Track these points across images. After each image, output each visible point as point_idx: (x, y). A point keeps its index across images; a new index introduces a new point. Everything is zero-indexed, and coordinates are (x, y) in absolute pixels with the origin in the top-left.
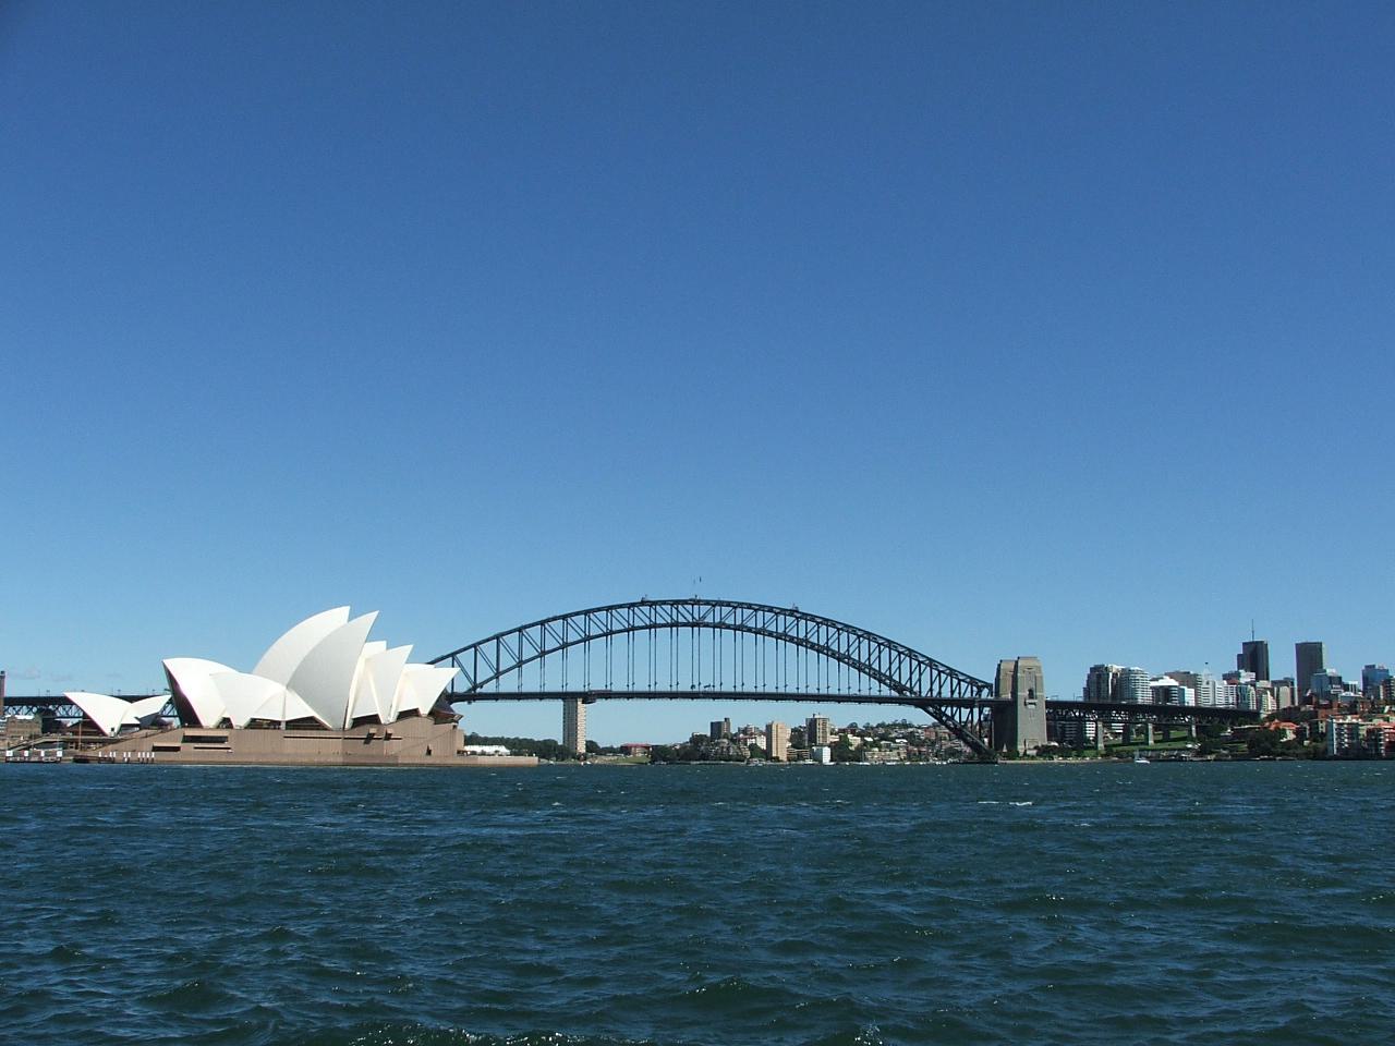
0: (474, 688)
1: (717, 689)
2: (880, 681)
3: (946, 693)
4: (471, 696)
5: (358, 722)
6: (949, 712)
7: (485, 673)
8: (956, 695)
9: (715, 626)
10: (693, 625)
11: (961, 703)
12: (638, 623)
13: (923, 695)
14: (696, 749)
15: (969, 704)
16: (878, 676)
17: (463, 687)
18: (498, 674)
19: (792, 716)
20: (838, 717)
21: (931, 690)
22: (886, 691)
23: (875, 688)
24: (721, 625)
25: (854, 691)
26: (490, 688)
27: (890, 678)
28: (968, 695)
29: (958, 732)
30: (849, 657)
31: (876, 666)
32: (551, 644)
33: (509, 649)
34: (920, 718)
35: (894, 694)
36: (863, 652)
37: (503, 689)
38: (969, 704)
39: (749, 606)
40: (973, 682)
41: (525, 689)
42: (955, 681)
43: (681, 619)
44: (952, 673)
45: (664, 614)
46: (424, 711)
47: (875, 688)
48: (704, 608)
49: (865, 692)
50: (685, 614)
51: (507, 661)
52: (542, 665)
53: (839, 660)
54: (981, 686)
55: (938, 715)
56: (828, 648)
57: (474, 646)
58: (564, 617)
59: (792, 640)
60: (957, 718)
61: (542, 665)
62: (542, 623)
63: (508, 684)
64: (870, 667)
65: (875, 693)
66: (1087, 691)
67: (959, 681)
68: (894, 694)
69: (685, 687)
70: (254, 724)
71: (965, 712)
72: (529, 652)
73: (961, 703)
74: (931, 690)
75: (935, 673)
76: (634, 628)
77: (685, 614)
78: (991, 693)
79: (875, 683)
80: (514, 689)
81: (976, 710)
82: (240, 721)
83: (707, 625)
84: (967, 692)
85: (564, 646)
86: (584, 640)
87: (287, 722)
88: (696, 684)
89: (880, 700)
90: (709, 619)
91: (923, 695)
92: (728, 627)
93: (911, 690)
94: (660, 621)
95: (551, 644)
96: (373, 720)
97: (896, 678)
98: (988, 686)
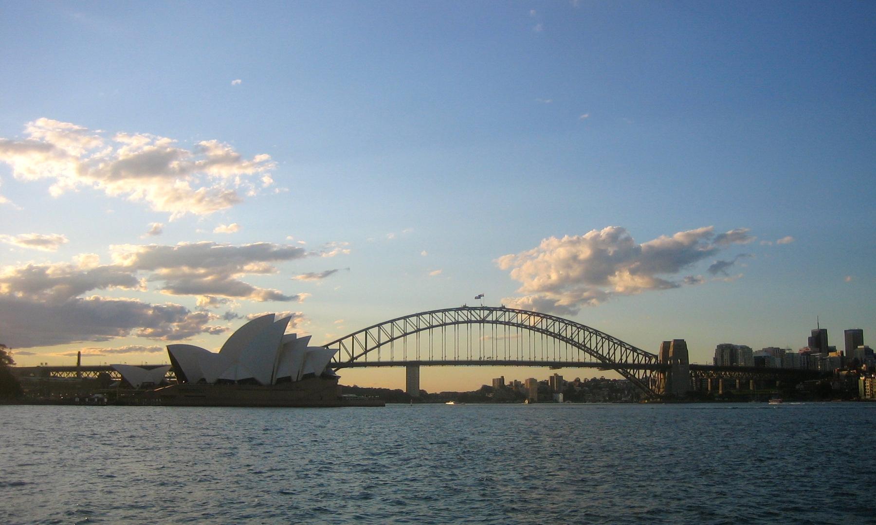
0: (353, 358)
1: (495, 359)
2: (591, 354)
3: (630, 361)
4: (351, 364)
5: (280, 381)
6: (632, 372)
7: (358, 351)
8: (636, 362)
9: (493, 322)
10: (479, 322)
11: (639, 367)
12: (448, 321)
13: (617, 361)
14: (483, 396)
15: (645, 367)
17: (345, 358)
18: (366, 352)
19: (543, 374)
20: (569, 375)
21: (621, 359)
22: (594, 360)
23: (588, 358)
24: (497, 322)
25: (575, 360)
26: (362, 359)
27: (597, 352)
28: (643, 362)
30: (572, 340)
31: (588, 345)
33: (373, 338)
34: (612, 375)
35: (599, 361)
36: (581, 337)
37: (369, 360)
38: (645, 367)
39: (513, 311)
40: (646, 354)
41: (382, 360)
42: (635, 354)
43: (473, 319)
44: (634, 350)
45: (463, 315)
46: (319, 373)
47: (588, 358)
48: (487, 312)
49: (582, 360)
50: (476, 315)
51: (371, 344)
52: (392, 346)
53: (567, 342)
55: (625, 374)
56: (560, 335)
57: (353, 335)
58: (405, 318)
59: (538, 330)
60: (637, 376)
61: (392, 346)
62: (392, 321)
63: (372, 357)
64: (585, 346)
65: (588, 360)
66: (715, 359)
67: (638, 354)
68: (599, 361)
69: (476, 358)
70: (220, 382)
71: (642, 372)
72: (384, 338)
73: (639, 367)
74: (621, 359)
75: (623, 349)
76: (445, 324)
77: (476, 315)
78: (657, 359)
79: (587, 355)
80: (376, 360)
81: (648, 372)
82: (211, 379)
83: (488, 322)
84: (643, 360)
85: (405, 334)
86: (416, 331)
87: (239, 381)
88: (482, 356)
90: (489, 318)
91: (617, 361)
92: (501, 323)
93: (609, 359)
94: (461, 320)
96: (288, 379)
97: (600, 352)
98: (656, 357)
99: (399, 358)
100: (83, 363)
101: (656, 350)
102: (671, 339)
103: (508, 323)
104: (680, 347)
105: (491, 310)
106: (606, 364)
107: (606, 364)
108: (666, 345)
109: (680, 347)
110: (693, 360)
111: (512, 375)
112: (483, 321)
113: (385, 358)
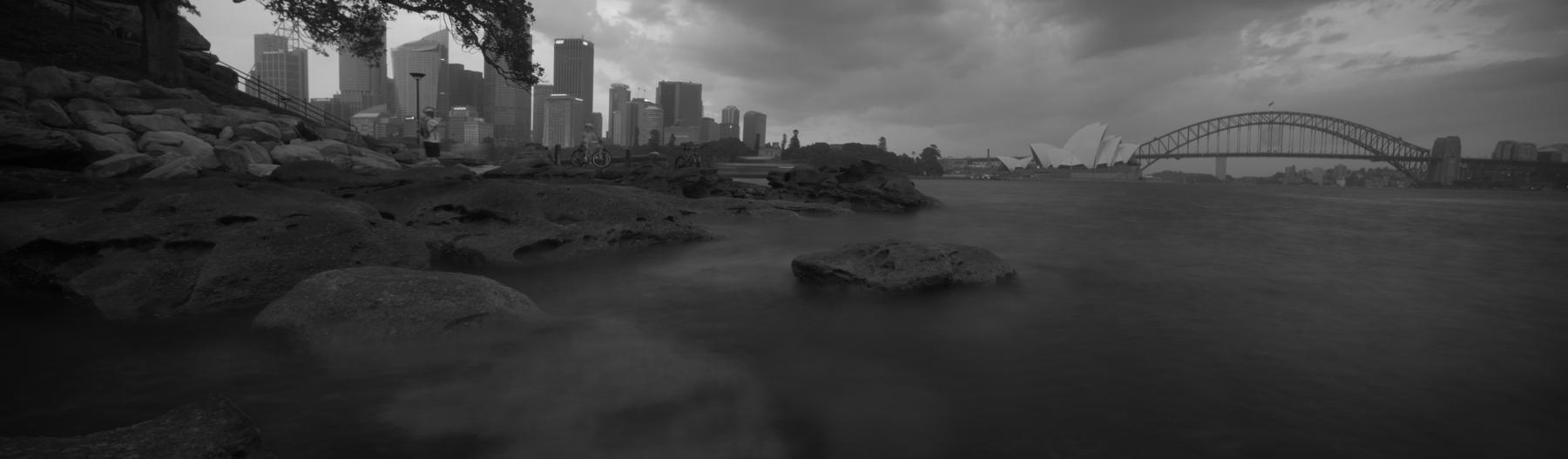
4: (1167, 155)
7: (1172, 146)
11: (1410, 159)
15: (1416, 159)
16: (1366, 147)
17: (1163, 152)
20: (1354, 165)
23: (1362, 151)
29: (1408, 173)
32: (1202, 133)
36: (1357, 135)
38: (1416, 159)
40: (1418, 149)
44: (1406, 144)
47: (1362, 151)
51: (1182, 141)
54: (1423, 151)
63: (1183, 150)
66: (1494, 154)
72: (1192, 136)
73: (1410, 159)
77: (1267, 118)
89: (1365, 157)
95: (1202, 133)
99: (1203, 151)
100: (992, 156)
101: (1428, 144)
102: (1444, 136)
103: (1293, 124)
104: (1455, 143)
105: (1279, 114)
106: (1378, 156)
107: (1378, 156)
108: (1440, 144)
109: (1455, 143)
110: (1465, 154)
111: (1302, 164)
112: (1271, 123)
113: (1192, 151)
